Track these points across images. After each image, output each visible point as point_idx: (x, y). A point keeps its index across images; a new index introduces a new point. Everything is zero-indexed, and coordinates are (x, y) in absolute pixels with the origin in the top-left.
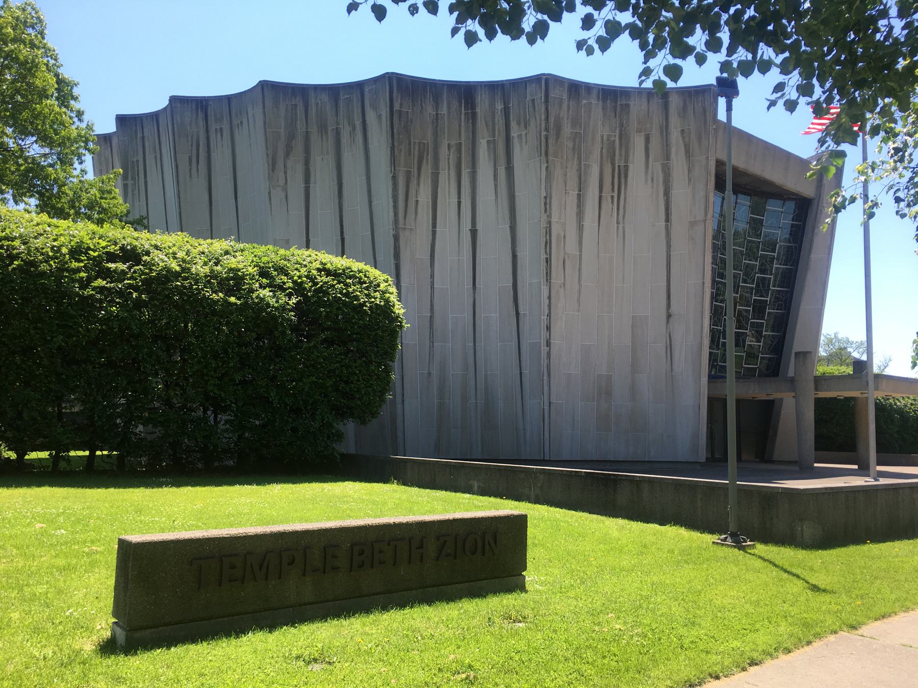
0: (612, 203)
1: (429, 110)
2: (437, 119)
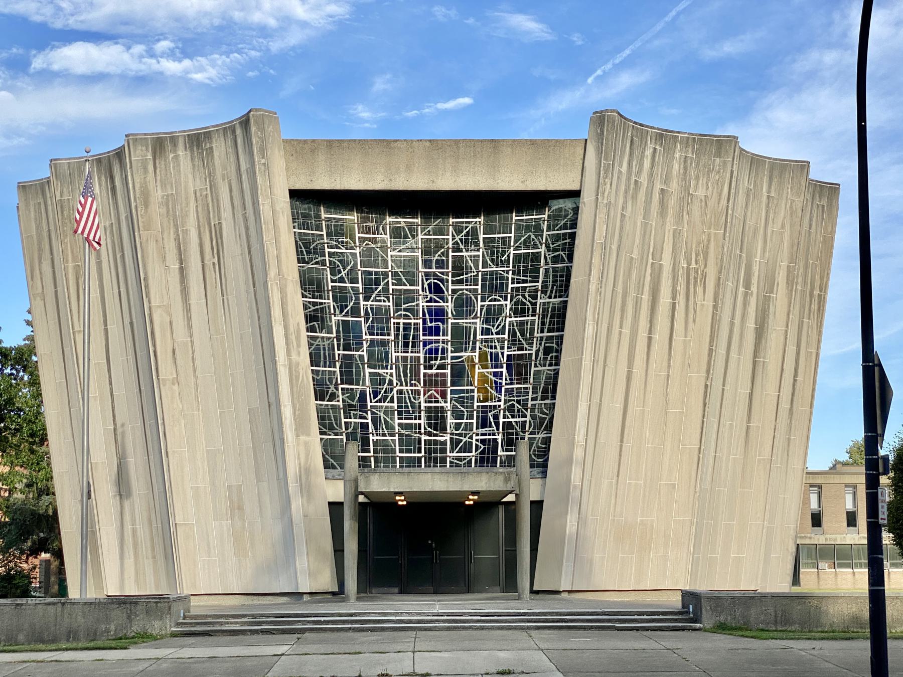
0: (215, 271)
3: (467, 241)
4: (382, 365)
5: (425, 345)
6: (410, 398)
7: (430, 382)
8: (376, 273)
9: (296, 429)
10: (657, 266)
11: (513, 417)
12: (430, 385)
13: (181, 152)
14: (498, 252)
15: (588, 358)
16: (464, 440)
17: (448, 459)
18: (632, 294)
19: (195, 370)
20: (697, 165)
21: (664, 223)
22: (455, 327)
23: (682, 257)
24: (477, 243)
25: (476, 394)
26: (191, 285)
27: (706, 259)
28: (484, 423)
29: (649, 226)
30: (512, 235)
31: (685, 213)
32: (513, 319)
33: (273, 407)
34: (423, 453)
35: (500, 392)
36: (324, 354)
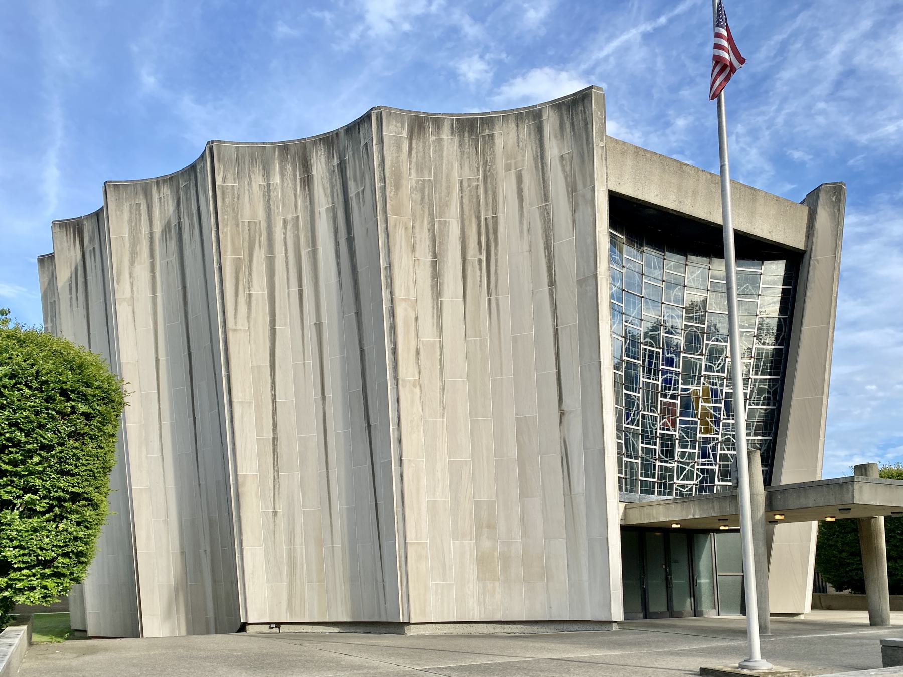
0: (480, 269)
1: (258, 179)
2: (269, 191)
11: (728, 450)
12: (664, 413)
16: (688, 468)
26: (446, 280)
28: (704, 455)
35: (719, 426)
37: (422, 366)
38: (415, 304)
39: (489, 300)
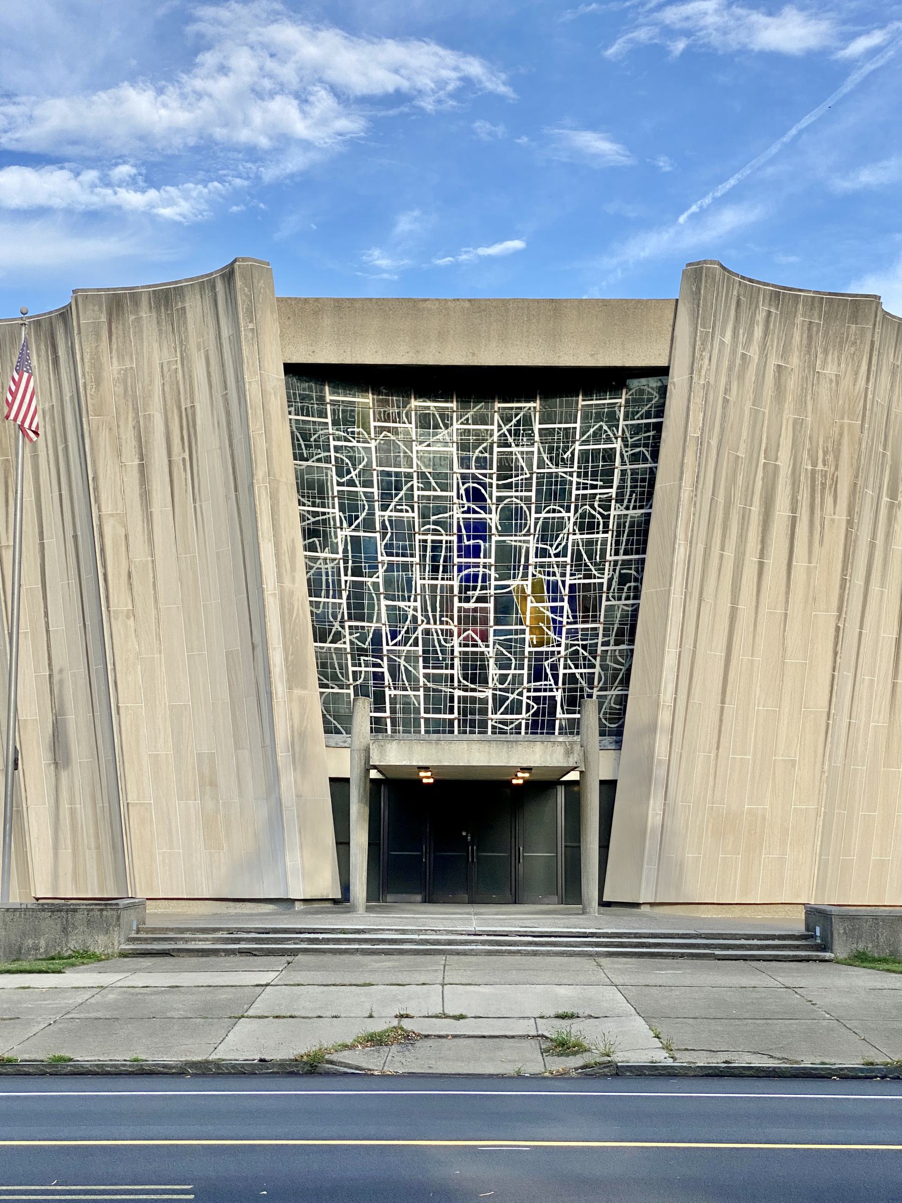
0: (185, 469)
3: (517, 433)
4: (403, 596)
5: (460, 570)
6: (439, 640)
7: (466, 619)
8: (397, 474)
9: (288, 680)
10: (770, 468)
11: (576, 667)
13: (144, 313)
14: (558, 448)
15: (678, 589)
16: (511, 697)
17: (490, 723)
18: (738, 505)
19: (156, 600)
20: (826, 334)
21: (781, 411)
22: (501, 546)
23: (806, 456)
24: (530, 436)
25: (527, 636)
26: (154, 487)
27: (837, 458)
28: (538, 674)
29: (761, 414)
30: (578, 425)
31: (809, 398)
32: (578, 536)
33: (259, 650)
34: (456, 715)
35: (560, 633)
36: (327, 580)
37: (135, 593)
38: (123, 520)
39: (195, 507)
